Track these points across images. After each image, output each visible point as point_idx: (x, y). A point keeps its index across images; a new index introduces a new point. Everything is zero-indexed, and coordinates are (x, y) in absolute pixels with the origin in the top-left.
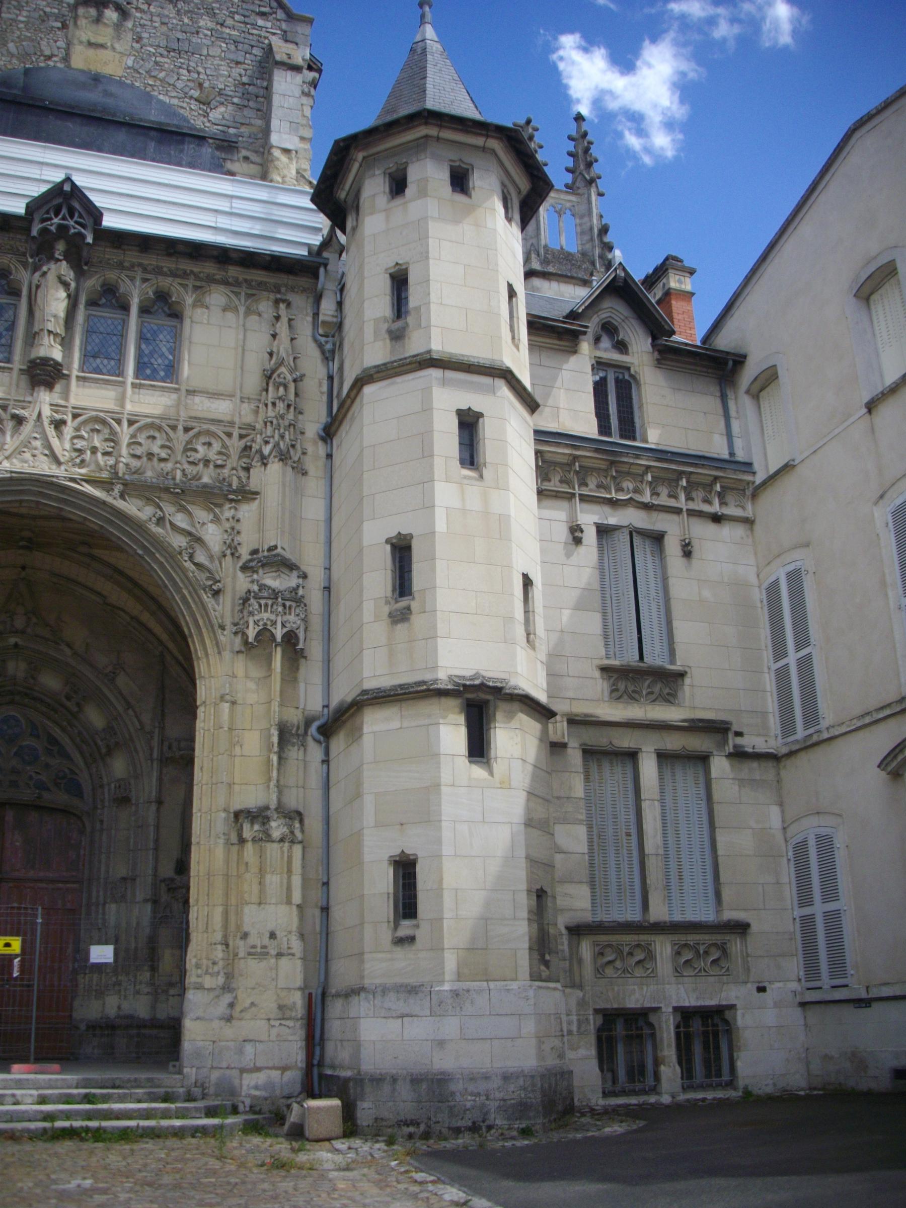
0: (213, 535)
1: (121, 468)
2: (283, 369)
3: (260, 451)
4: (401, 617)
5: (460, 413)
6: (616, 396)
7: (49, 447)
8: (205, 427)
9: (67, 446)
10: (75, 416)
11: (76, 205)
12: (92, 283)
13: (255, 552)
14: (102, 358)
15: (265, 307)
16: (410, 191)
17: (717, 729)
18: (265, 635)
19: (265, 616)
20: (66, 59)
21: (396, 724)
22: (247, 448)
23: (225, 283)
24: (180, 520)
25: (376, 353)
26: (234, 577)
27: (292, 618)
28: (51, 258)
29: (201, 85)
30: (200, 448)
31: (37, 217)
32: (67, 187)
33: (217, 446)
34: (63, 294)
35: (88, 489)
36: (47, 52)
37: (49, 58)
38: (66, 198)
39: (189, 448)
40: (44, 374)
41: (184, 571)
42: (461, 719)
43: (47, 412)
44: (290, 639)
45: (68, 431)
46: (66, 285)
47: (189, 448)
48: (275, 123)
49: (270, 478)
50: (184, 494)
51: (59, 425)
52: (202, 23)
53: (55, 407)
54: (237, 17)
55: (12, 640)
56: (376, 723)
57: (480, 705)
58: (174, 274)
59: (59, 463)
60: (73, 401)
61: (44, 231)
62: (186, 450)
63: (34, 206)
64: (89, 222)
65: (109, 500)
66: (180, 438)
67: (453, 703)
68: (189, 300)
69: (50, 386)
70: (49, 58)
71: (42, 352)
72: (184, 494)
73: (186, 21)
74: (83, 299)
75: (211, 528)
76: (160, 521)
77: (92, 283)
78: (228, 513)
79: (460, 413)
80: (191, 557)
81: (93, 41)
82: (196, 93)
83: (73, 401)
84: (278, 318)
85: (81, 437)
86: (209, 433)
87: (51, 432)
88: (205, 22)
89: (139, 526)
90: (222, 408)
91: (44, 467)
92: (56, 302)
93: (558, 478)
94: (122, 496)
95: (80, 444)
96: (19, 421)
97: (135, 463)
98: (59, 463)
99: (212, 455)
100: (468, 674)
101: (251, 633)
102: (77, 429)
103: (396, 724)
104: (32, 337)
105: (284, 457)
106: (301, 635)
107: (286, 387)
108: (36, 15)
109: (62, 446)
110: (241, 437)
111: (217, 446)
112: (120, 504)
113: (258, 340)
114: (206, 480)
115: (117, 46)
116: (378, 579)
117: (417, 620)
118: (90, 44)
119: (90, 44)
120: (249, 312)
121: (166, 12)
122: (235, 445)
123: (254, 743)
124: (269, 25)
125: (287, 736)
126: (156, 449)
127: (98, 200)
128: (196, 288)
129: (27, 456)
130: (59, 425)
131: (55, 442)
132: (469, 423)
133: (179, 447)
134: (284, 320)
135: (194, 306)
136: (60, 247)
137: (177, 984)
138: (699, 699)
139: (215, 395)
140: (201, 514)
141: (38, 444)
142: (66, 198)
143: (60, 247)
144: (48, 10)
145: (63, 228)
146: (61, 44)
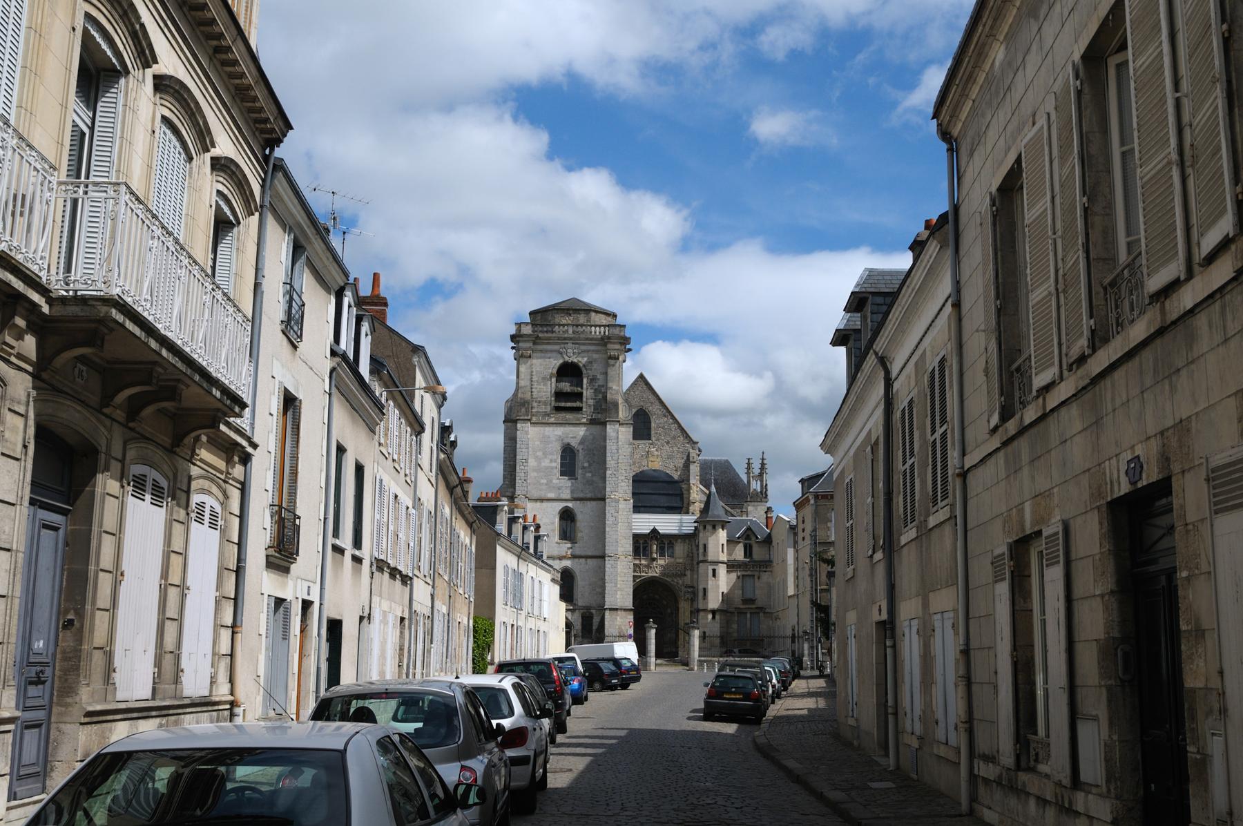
6: (748, 551)
14: (662, 555)
17: (761, 608)
25: (701, 558)
38: (654, 531)
40: (654, 559)
49: (688, 573)
50: (676, 575)
56: (701, 614)
57: (714, 612)
72: (676, 575)
116: (701, 594)
123: (688, 614)
125: (691, 612)
132: (714, 571)
137: (677, 648)
138: (759, 603)
142: (654, 531)
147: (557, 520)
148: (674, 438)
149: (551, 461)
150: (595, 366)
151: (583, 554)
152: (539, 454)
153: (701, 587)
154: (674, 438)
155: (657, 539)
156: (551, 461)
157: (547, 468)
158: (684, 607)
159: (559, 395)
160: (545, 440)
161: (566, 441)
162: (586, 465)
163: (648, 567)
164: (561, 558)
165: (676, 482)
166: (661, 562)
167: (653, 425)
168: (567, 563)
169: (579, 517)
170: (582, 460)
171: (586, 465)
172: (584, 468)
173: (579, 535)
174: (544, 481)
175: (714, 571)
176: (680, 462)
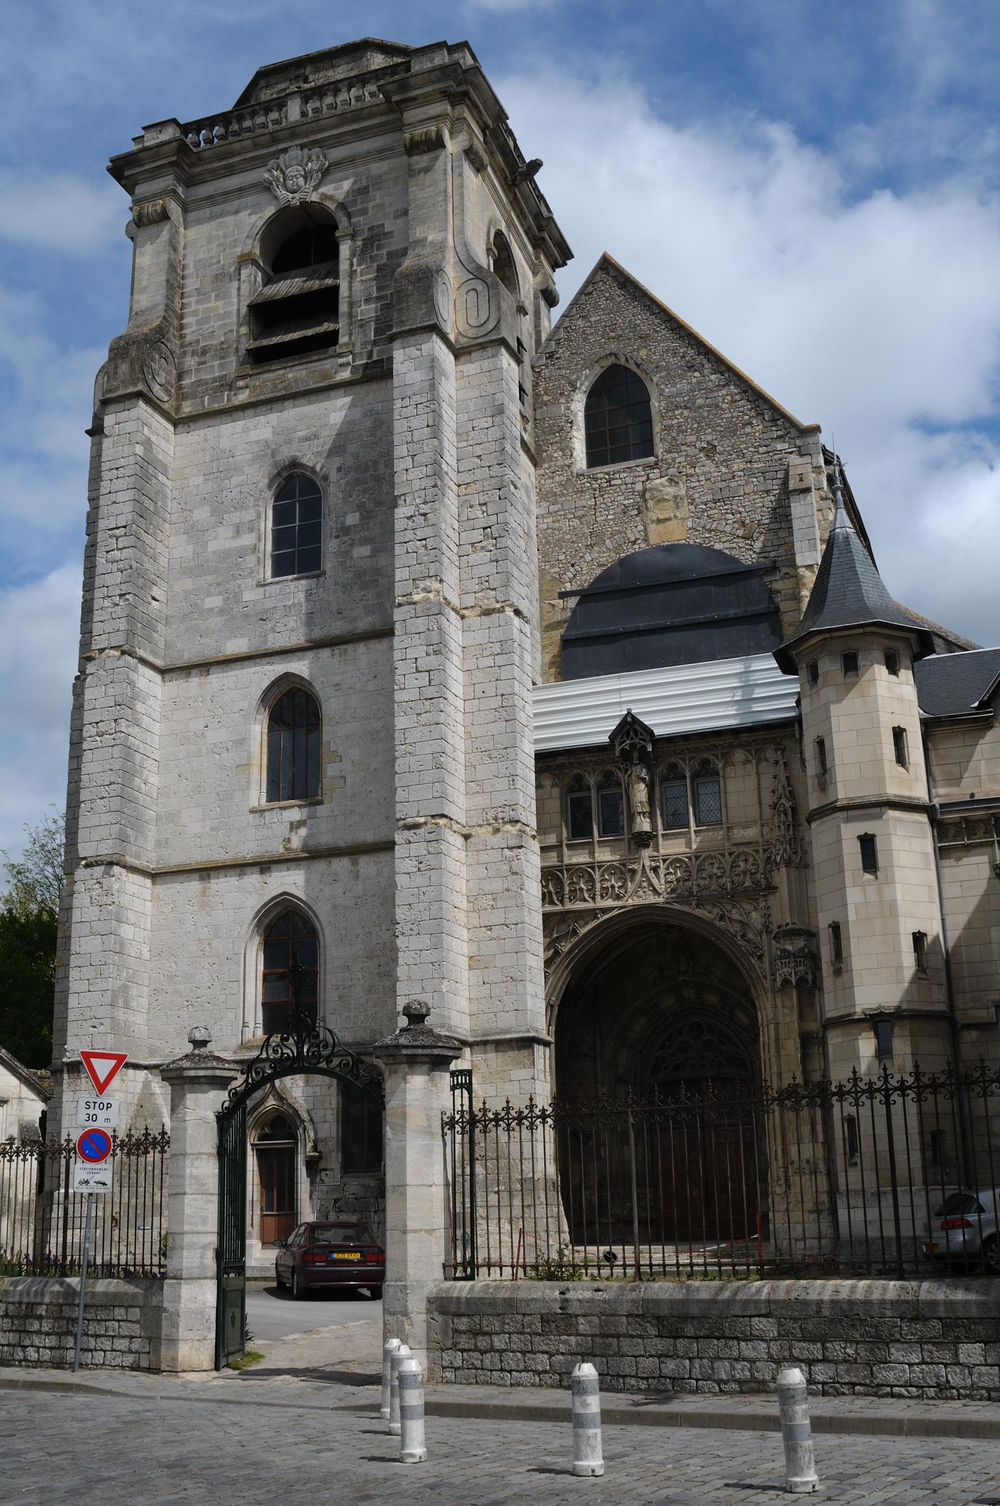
0: (756, 918)
1: (695, 889)
2: (783, 801)
3: (775, 860)
4: (838, 972)
5: (860, 838)
7: (651, 884)
8: (742, 849)
9: (663, 881)
10: (664, 861)
11: (637, 727)
12: (661, 769)
13: (779, 927)
15: (770, 754)
16: (820, 681)
18: (786, 982)
19: (785, 970)
20: (646, 540)
21: (840, 1039)
22: (769, 858)
23: (741, 746)
24: (735, 915)
25: (814, 802)
26: (770, 945)
27: (802, 968)
28: (632, 763)
29: (743, 524)
30: (741, 864)
31: (617, 743)
32: (629, 719)
33: (751, 860)
34: (642, 786)
35: (677, 906)
36: (632, 539)
37: (634, 543)
38: (630, 726)
39: (734, 866)
40: (644, 840)
41: (740, 946)
42: (872, 1034)
43: (647, 863)
44: (801, 981)
45: (662, 871)
46: (643, 780)
47: (734, 866)
48: (797, 545)
49: (781, 877)
50: (735, 896)
51: (655, 870)
52: (735, 467)
53: (652, 858)
54: (761, 450)
55: (681, 978)
58: (708, 749)
59: (659, 894)
60: (662, 851)
61: (622, 750)
62: (732, 867)
63: (613, 736)
64: (648, 738)
65: (690, 911)
66: (729, 859)
67: (865, 1025)
68: (721, 765)
69: (647, 846)
70: (634, 543)
71: (637, 829)
73: (724, 470)
74: (657, 783)
75: (754, 915)
76: (722, 918)
77: (661, 769)
78: (762, 904)
79: (860, 838)
80: (743, 936)
81: (661, 517)
82: (740, 532)
83: (662, 851)
84: (776, 762)
85: (670, 873)
86: (744, 853)
87: (652, 875)
88: (738, 465)
89: (710, 924)
90: (752, 833)
91: (652, 899)
92: (640, 793)
93: (982, 830)
94: (698, 906)
95: (670, 878)
96: (633, 872)
97: (702, 882)
98: (659, 894)
99: (750, 867)
100: (874, 1006)
101: (779, 981)
102: (667, 869)
103: (840, 1039)
104: (631, 819)
105: (788, 863)
106: (810, 978)
107: (786, 815)
108: (619, 510)
109: (660, 885)
110: (765, 851)
111: (751, 860)
112: (699, 912)
113: (767, 782)
114: (747, 884)
115: (678, 514)
117: (845, 975)
118: (659, 521)
119: (659, 521)
120: (759, 761)
121: (706, 469)
122: (761, 858)
124: (786, 446)
126: (715, 871)
127: (647, 721)
128: (723, 755)
129: (641, 893)
130: (655, 870)
131: (655, 881)
133: (728, 868)
134: (781, 763)
135: (724, 767)
136: (635, 755)
139: (746, 826)
140: (748, 907)
141: (645, 884)
142: (630, 726)
143: (635, 755)
144: (626, 502)
145: (633, 746)
146: (641, 528)
147: (258, 730)
148: (731, 431)
149: (238, 531)
150: (377, 197)
151: (343, 838)
152: (202, 514)
153: (823, 922)
154: (731, 431)
155: (645, 759)
156: (238, 531)
157: (224, 555)
158: (777, 1018)
159: (265, 315)
160: (219, 466)
161: (286, 453)
162: (352, 519)
163: (624, 871)
164: (264, 865)
165: (750, 573)
166: (672, 847)
167: (655, 404)
168: (291, 881)
169: (330, 707)
170: (339, 507)
171: (352, 519)
172: (345, 530)
173: (330, 770)
174: (215, 602)
175: (867, 843)
176: (759, 508)
